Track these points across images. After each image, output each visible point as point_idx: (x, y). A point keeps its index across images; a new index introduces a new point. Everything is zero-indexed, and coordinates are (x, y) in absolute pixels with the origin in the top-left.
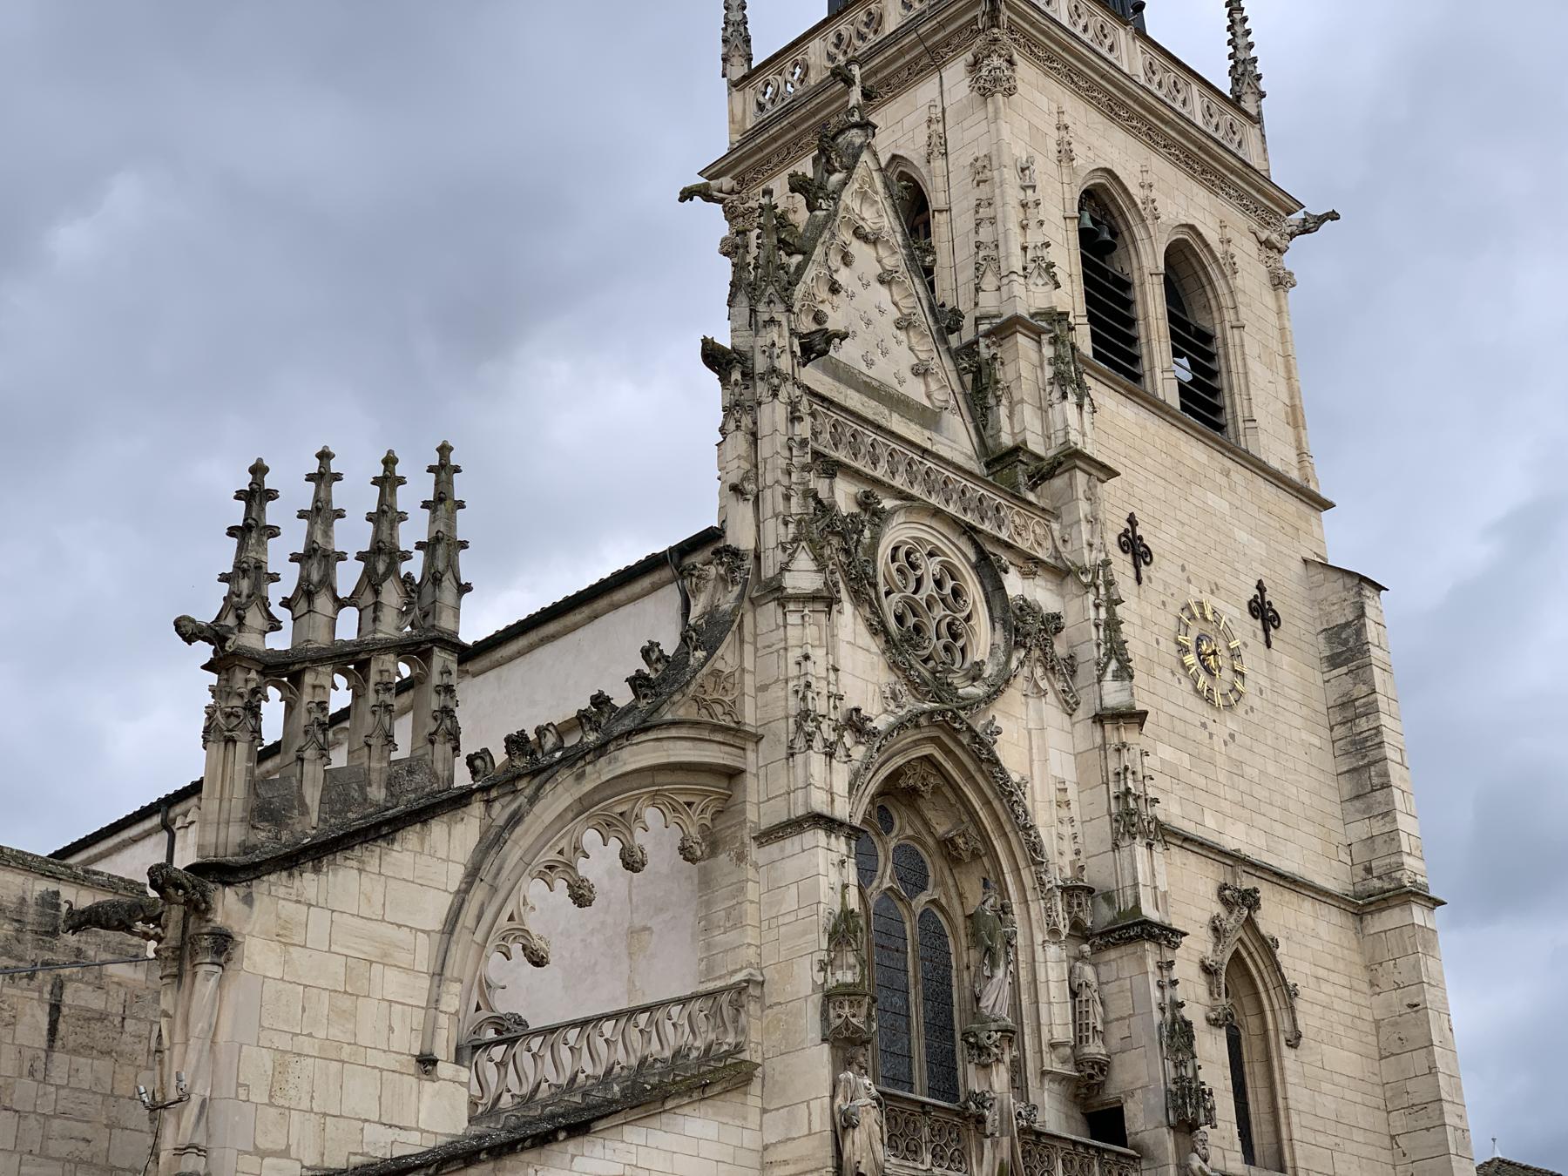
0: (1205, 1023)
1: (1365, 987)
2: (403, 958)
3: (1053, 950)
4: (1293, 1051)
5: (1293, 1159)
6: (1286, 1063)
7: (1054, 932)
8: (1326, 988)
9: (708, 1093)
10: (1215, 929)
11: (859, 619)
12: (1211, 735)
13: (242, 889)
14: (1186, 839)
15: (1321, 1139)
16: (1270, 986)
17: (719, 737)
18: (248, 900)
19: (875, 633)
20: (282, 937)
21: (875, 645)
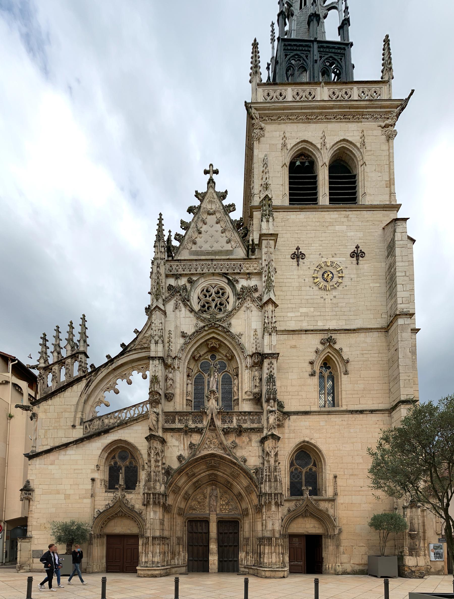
0: (308, 376)
1: (386, 351)
2: (69, 410)
3: (247, 371)
4: (346, 376)
5: (342, 403)
6: (342, 379)
7: (247, 367)
8: (365, 356)
9: (138, 421)
10: (316, 352)
11: (187, 311)
12: (325, 300)
13: (37, 406)
14: (306, 331)
15: (354, 396)
16: (339, 361)
17: (144, 351)
18: (39, 407)
19: (191, 312)
20: (45, 412)
21: (192, 315)
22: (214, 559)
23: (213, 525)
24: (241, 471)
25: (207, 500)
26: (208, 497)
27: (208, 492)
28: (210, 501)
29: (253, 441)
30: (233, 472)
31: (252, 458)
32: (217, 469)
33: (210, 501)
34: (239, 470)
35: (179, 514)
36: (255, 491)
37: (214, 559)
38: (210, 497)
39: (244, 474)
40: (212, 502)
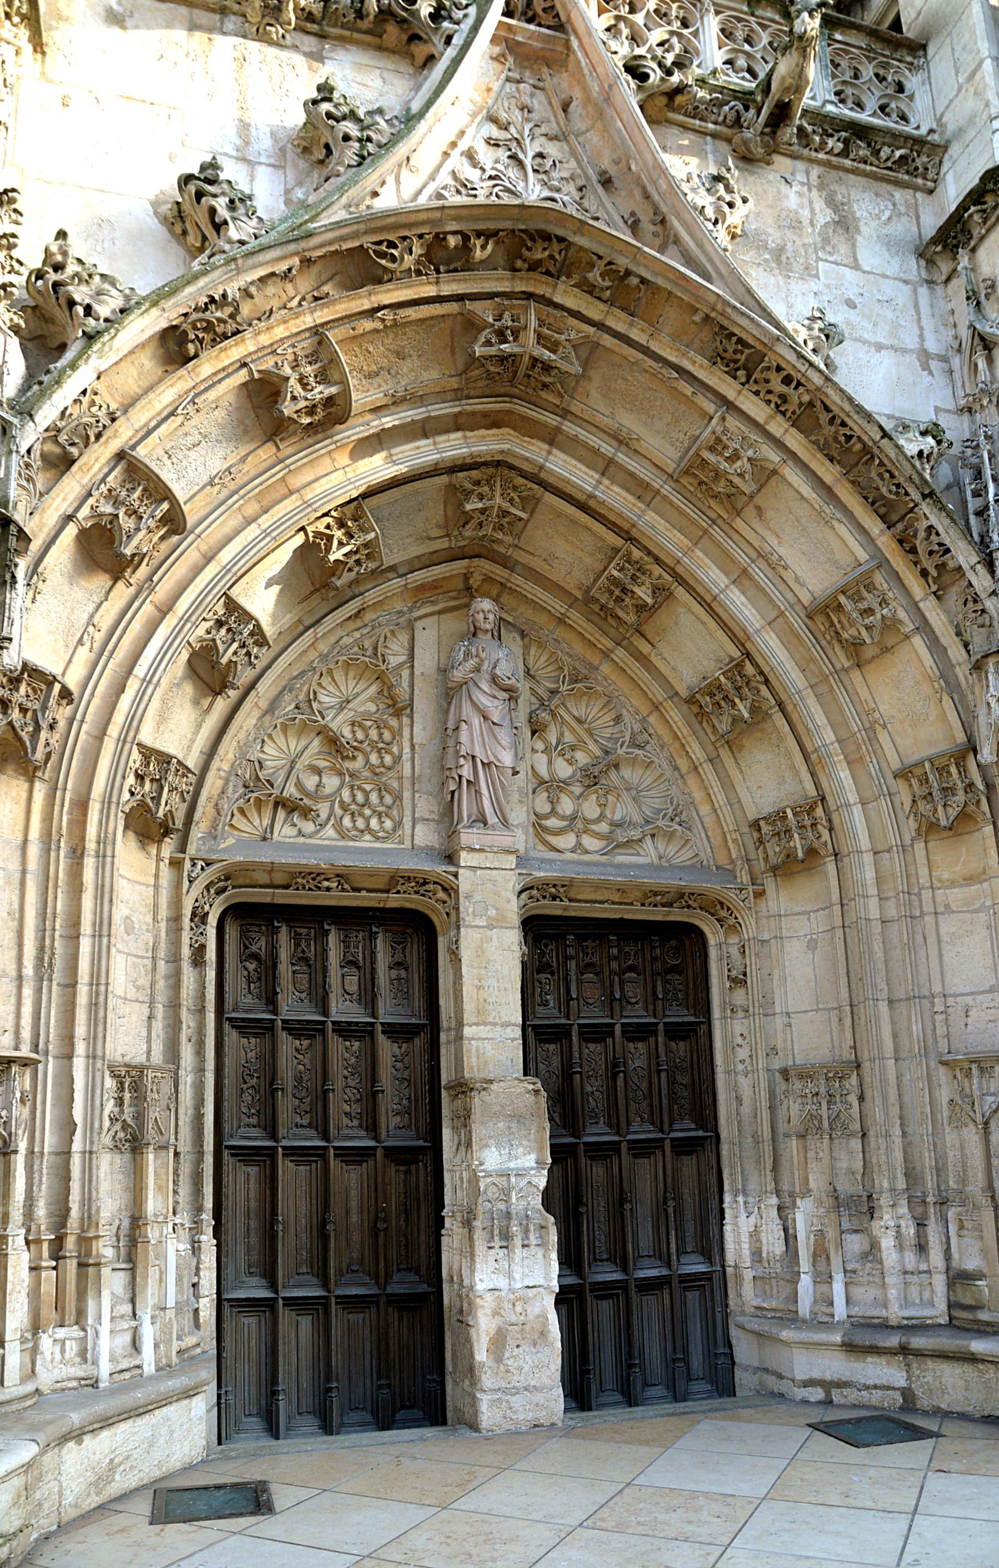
22: (508, 1287)
23: (492, 949)
24: (794, 440)
25: (422, 728)
26: (424, 706)
27: (426, 660)
28: (447, 734)
29: (868, 230)
30: (717, 446)
31: (876, 357)
32: (552, 420)
33: (447, 734)
34: (778, 427)
35: (147, 826)
36: (924, 627)
37: (508, 1287)
38: (450, 693)
39: (829, 472)
40: (472, 737)
